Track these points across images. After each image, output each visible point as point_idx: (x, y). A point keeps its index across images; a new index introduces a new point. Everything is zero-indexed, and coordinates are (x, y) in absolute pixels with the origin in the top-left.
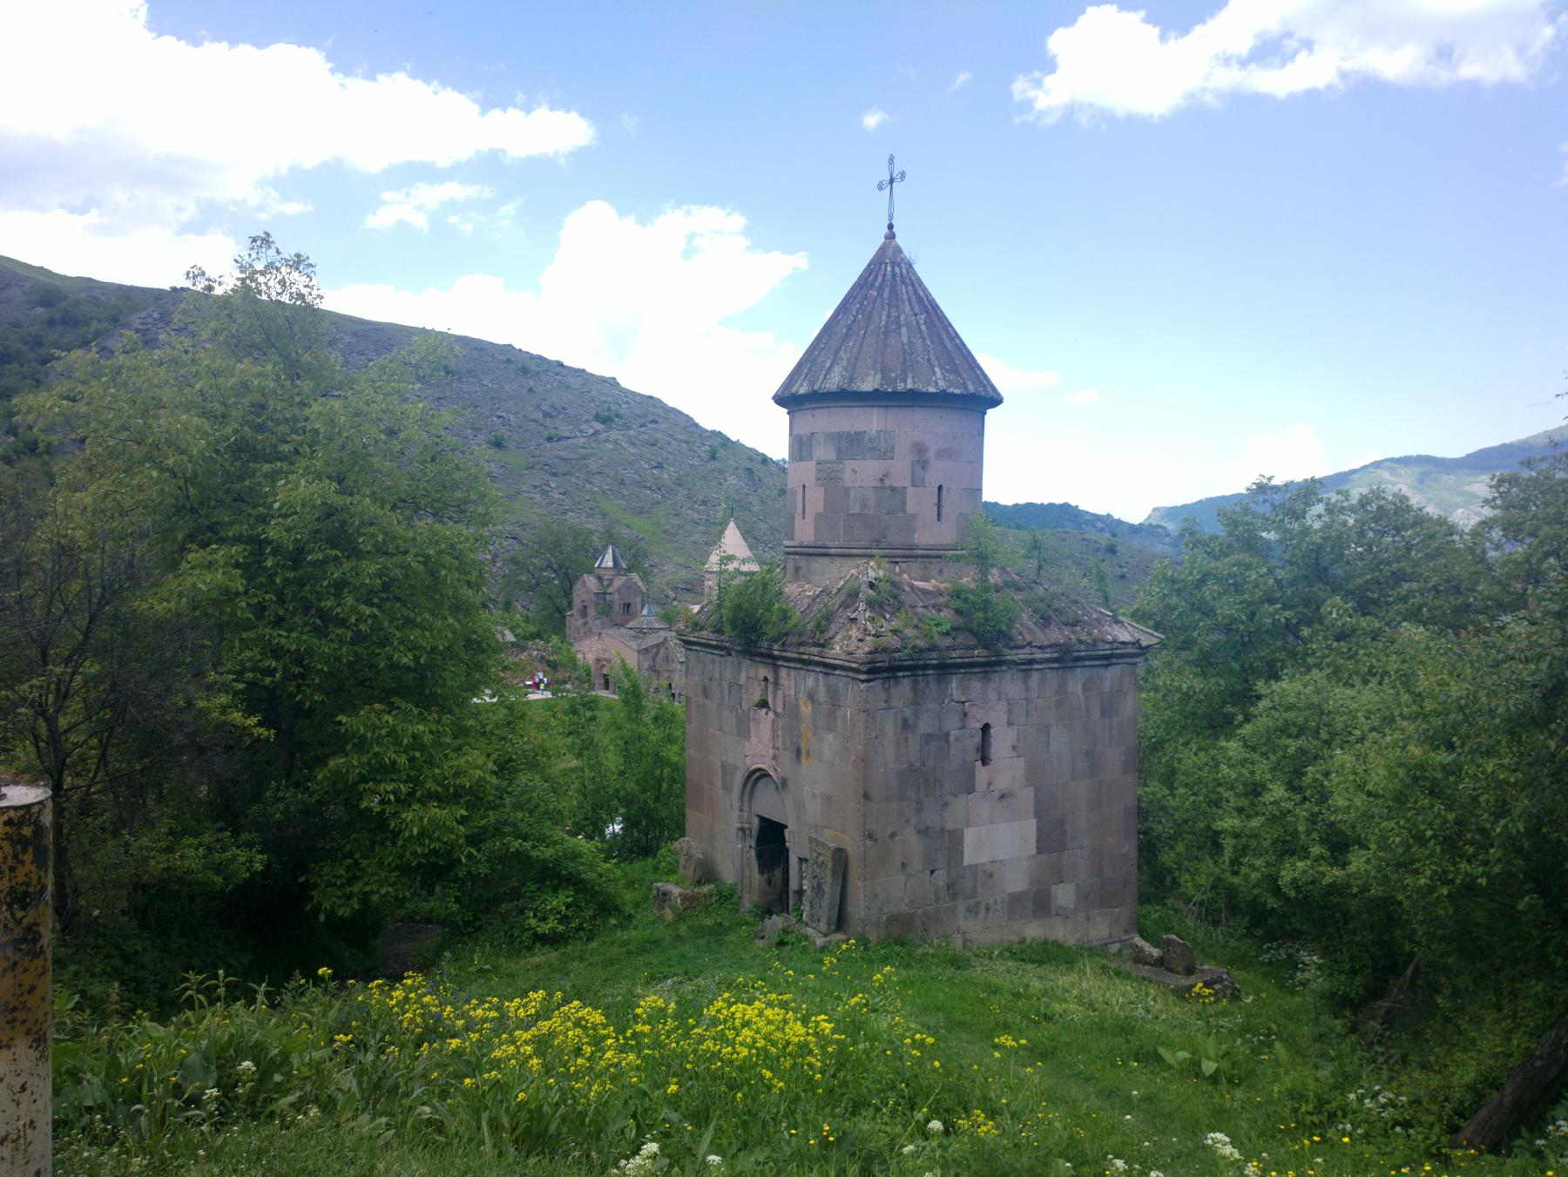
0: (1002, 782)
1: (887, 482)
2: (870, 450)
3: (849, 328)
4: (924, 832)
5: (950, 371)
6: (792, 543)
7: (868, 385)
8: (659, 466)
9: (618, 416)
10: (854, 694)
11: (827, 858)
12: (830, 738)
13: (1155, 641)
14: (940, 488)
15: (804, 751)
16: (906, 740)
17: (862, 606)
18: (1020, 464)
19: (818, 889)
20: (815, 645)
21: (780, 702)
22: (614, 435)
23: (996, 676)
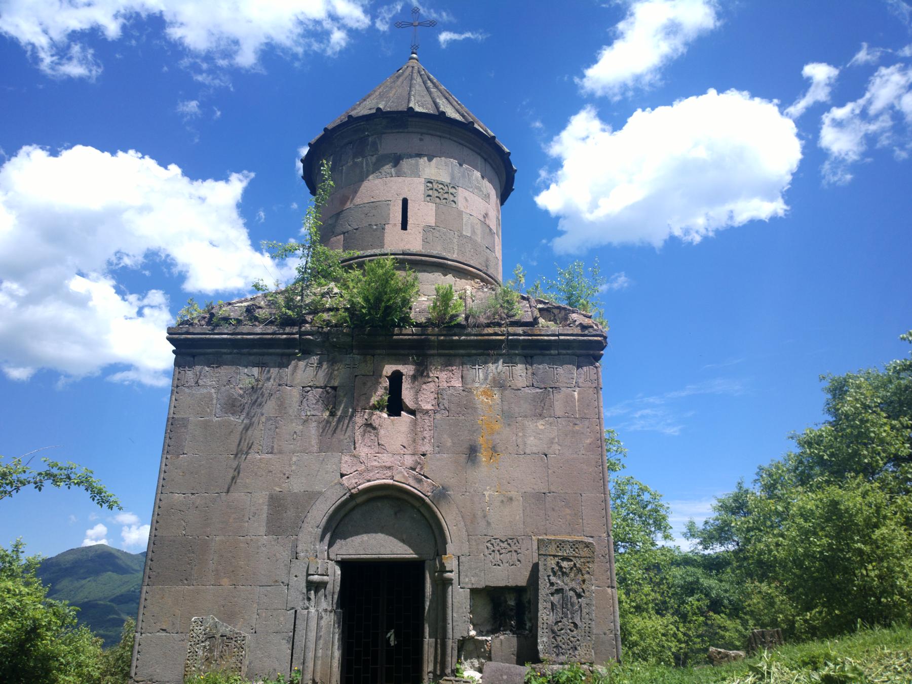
12: (541, 425)
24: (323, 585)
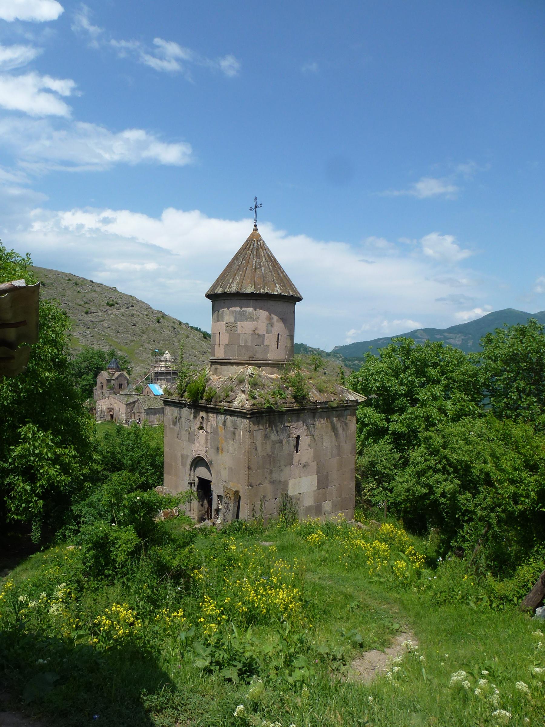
0: (304, 460)
1: (256, 332)
2: (249, 318)
3: (239, 266)
4: (273, 482)
5: (282, 286)
6: (214, 358)
7: (249, 290)
8: (134, 325)
9: (117, 303)
10: (244, 424)
11: (231, 495)
13: (364, 400)
14: (278, 334)
15: (220, 449)
16: (266, 443)
17: (247, 385)
18: (320, 327)
19: (228, 508)
20: (226, 402)
21: (209, 427)
22: (115, 311)
23: (302, 415)
24: (194, 483)
